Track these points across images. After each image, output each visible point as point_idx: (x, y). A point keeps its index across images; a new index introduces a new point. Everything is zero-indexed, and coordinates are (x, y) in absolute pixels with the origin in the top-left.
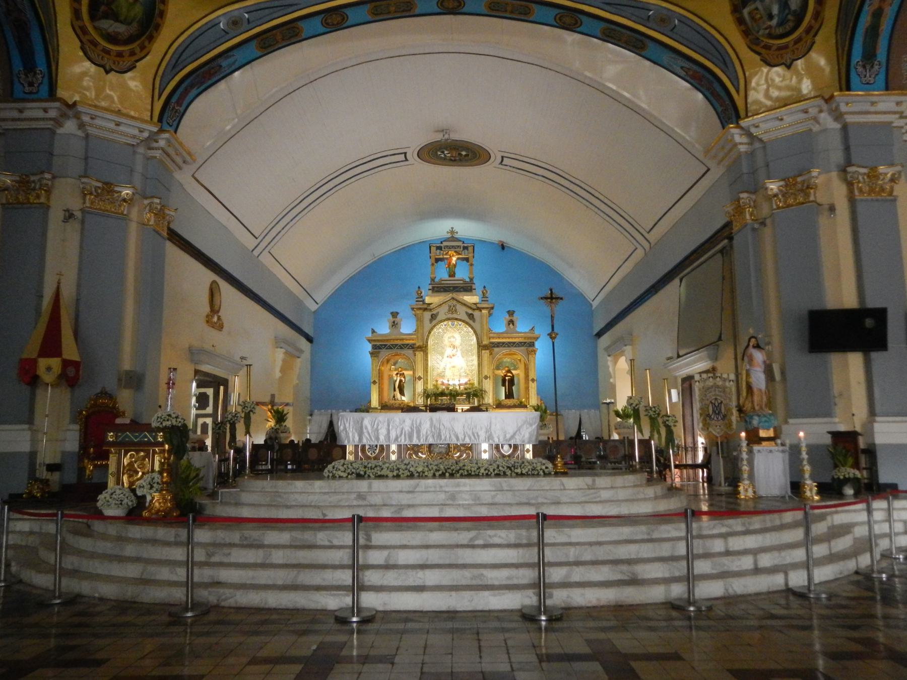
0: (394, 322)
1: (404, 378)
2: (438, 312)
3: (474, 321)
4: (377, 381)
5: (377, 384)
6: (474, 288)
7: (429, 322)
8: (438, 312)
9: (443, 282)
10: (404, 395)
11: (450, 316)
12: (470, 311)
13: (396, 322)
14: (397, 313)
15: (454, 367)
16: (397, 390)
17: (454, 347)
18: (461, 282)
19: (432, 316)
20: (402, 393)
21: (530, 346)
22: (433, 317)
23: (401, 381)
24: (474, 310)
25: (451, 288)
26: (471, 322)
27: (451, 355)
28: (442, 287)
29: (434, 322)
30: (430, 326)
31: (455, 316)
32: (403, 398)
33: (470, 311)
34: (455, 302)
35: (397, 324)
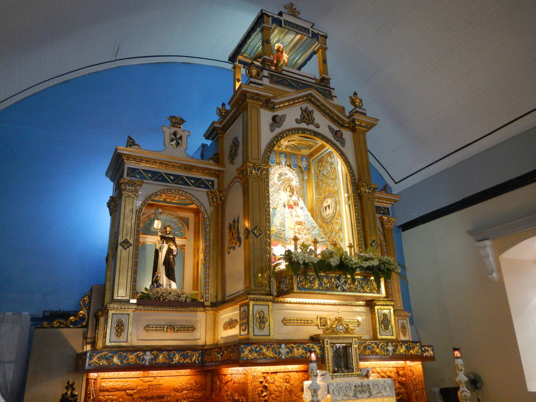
0: (175, 134)
1: (176, 246)
2: (285, 115)
3: (343, 144)
4: (131, 241)
5: (131, 248)
6: (333, 94)
7: (268, 128)
8: (285, 115)
9: (284, 72)
10: (174, 280)
11: (303, 125)
12: (336, 128)
13: (178, 136)
14: (182, 121)
15: (300, 223)
16: (162, 269)
17: (292, 190)
18: (313, 81)
19: (274, 118)
20: (170, 275)
21: (384, 214)
22: (276, 121)
23: (170, 251)
24: (342, 126)
25: (300, 85)
26: (338, 144)
27: (292, 203)
28: (285, 80)
29: (277, 131)
30: (271, 135)
31: (311, 127)
32: (174, 286)
33: (336, 128)
34: (311, 107)
35: (181, 138)
